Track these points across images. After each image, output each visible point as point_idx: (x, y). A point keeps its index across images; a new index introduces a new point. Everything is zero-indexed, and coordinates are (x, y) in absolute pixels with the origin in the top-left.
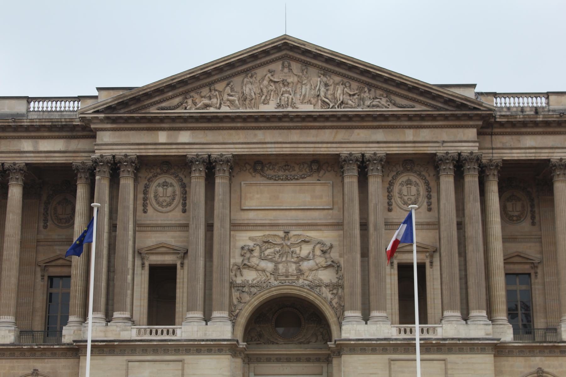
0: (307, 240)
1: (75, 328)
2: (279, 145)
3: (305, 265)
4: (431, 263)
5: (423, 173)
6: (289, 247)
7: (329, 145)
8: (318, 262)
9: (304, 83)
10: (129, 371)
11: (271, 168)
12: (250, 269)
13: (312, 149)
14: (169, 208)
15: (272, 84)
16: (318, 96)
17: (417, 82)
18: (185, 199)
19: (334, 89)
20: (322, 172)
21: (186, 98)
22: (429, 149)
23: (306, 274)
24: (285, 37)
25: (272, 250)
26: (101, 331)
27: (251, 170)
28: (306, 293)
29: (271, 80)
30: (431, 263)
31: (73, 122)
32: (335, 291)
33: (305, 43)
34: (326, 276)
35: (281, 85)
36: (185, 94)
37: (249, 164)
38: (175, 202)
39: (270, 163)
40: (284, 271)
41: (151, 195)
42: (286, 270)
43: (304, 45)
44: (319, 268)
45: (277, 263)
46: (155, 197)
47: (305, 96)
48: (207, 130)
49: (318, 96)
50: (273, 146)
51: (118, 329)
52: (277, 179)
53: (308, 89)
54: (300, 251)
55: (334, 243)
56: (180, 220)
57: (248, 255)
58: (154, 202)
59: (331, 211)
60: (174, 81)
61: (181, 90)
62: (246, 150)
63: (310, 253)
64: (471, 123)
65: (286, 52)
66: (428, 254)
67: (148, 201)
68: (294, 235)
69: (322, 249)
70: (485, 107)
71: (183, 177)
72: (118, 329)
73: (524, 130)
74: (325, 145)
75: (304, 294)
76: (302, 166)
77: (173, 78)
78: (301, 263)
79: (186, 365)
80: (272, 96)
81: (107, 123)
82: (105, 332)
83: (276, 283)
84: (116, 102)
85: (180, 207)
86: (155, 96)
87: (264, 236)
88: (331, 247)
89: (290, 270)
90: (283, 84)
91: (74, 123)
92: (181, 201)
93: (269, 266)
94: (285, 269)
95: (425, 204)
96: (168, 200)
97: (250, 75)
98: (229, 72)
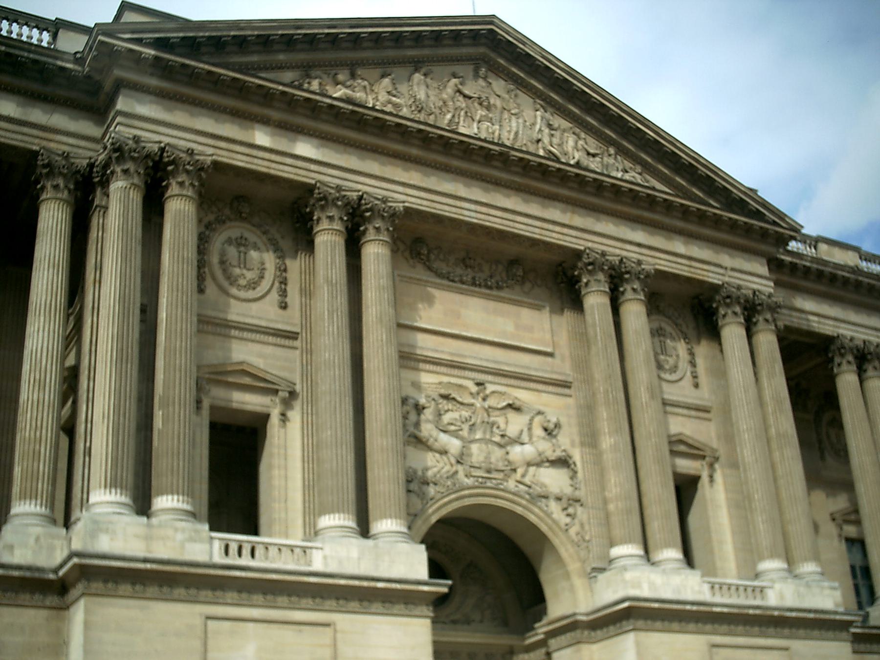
0: (518, 403)
1: (39, 530)
2: (484, 209)
3: (517, 452)
4: (711, 477)
5: (680, 321)
6: (488, 410)
7: (565, 231)
8: (541, 448)
9: (513, 112)
10: (211, 643)
11: (441, 256)
12: (420, 446)
13: (537, 230)
14: (251, 294)
15: (461, 98)
16: (538, 141)
17: (697, 158)
18: (284, 282)
19: (561, 139)
20: (528, 285)
21: (308, 76)
22: (711, 275)
23: (520, 471)
24: (490, 20)
25: (456, 415)
26: (136, 536)
27: (407, 254)
28: (524, 507)
29: (459, 91)
30: (711, 477)
31: (57, 58)
32: (571, 510)
33: (525, 40)
34: (554, 480)
35: (476, 104)
36: (307, 70)
37: (403, 242)
38: (265, 285)
39: (439, 248)
40: (481, 458)
41: (215, 260)
42: (486, 458)
43: (524, 44)
44: (541, 462)
45: (467, 443)
46: (222, 262)
47: (517, 133)
48: (351, 146)
49: (538, 141)
50: (472, 207)
51: (179, 536)
52: (456, 279)
53: (521, 125)
54: (507, 423)
55: (563, 420)
56: (277, 322)
57: (413, 417)
58: (219, 273)
59: (549, 359)
60: (299, 32)
61: (301, 57)
62: (425, 203)
63: (522, 431)
64: (763, 247)
65: (488, 48)
66: (704, 463)
67: (206, 270)
68: (493, 392)
69: (545, 425)
70: (787, 223)
71: (278, 236)
72: (179, 536)
73: (803, 283)
74: (558, 229)
75: (519, 510)
76: (494, 267)
77: (298, 23)
78: (509, 448)
79: (339, 636)
80: (462, 119)
81: (152, 75)
82: (148, 538)
83: (469, 481)
84: (181, 35)
85: (274, 296)
86: (253, 52)
87: (440, 383)
88: (557, 425)
89: (493, 460)
90: (481, 104)
91: (59, 63)
92: (277, 284)
93: (454, 445)
94: (484, 455)
95: (689, 374)
96: (250, 275)
97: (423, 70)
98: (391, 53)
